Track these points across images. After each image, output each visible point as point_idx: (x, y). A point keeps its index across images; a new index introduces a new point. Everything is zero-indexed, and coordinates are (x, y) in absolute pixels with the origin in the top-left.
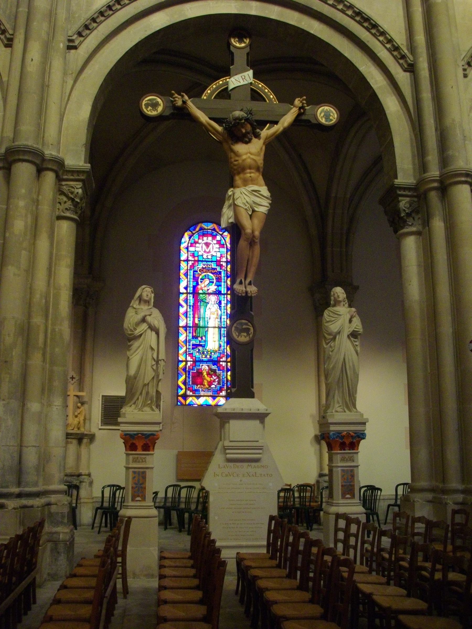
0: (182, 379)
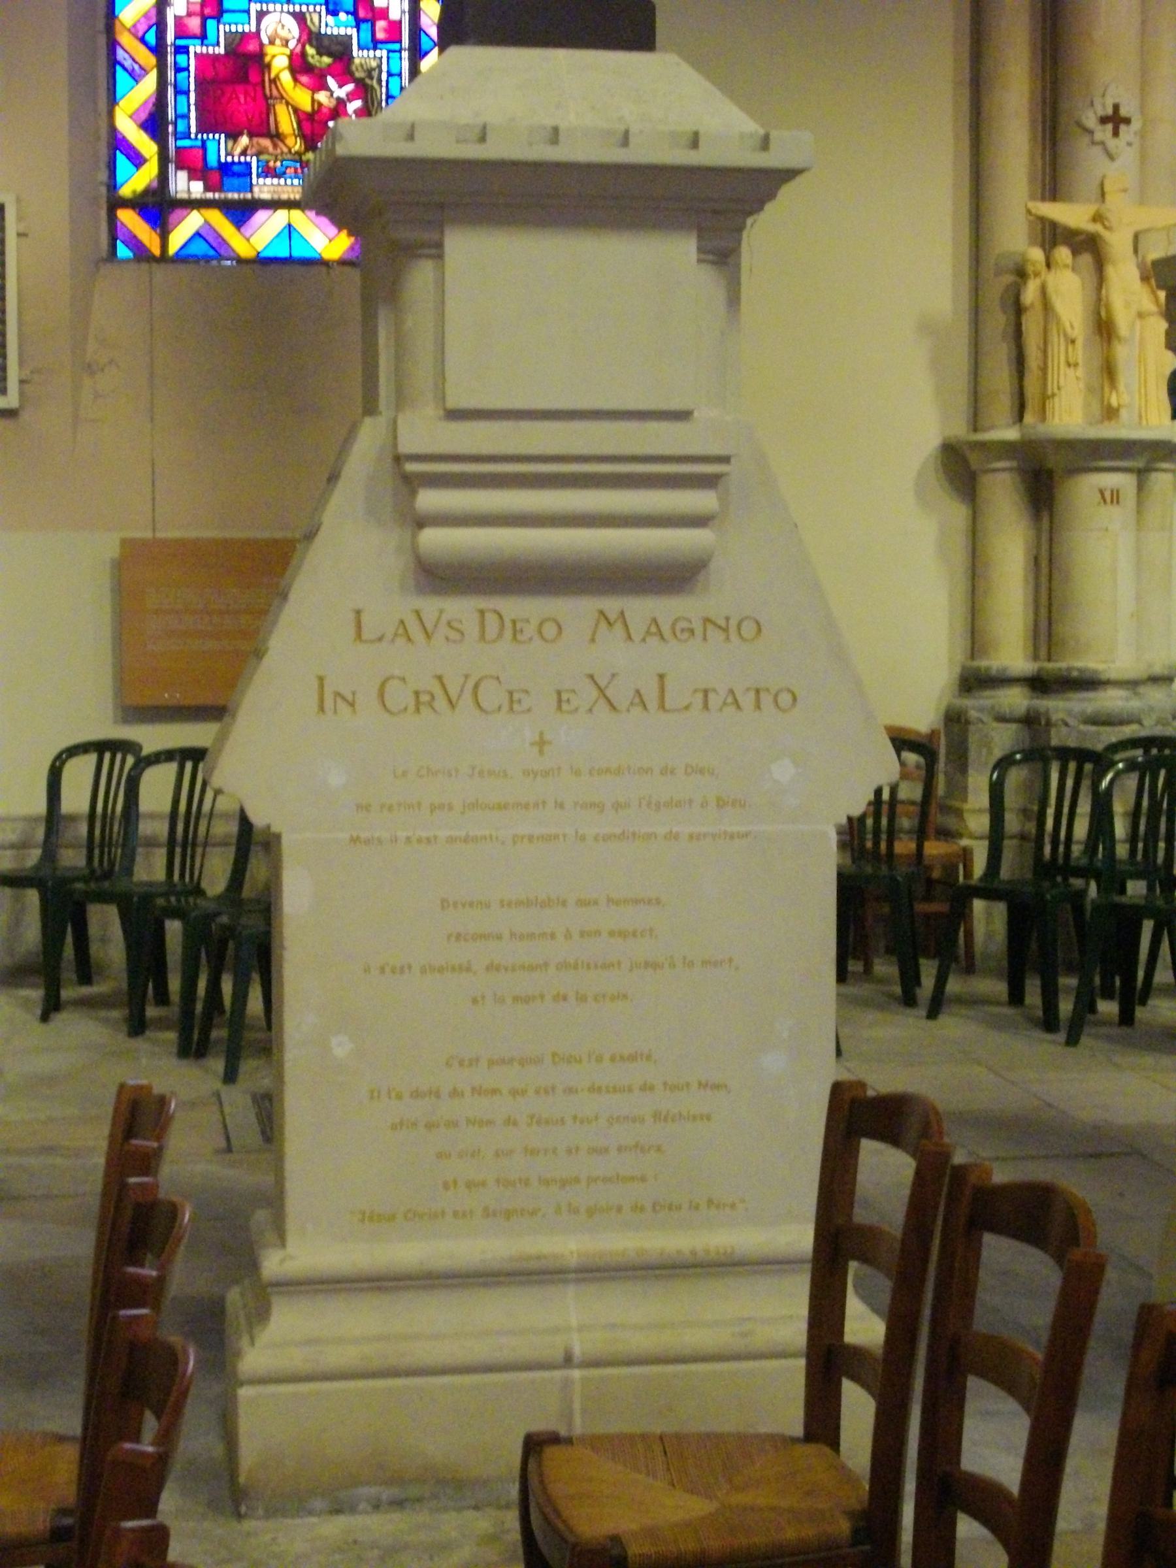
0: (136, 95)
